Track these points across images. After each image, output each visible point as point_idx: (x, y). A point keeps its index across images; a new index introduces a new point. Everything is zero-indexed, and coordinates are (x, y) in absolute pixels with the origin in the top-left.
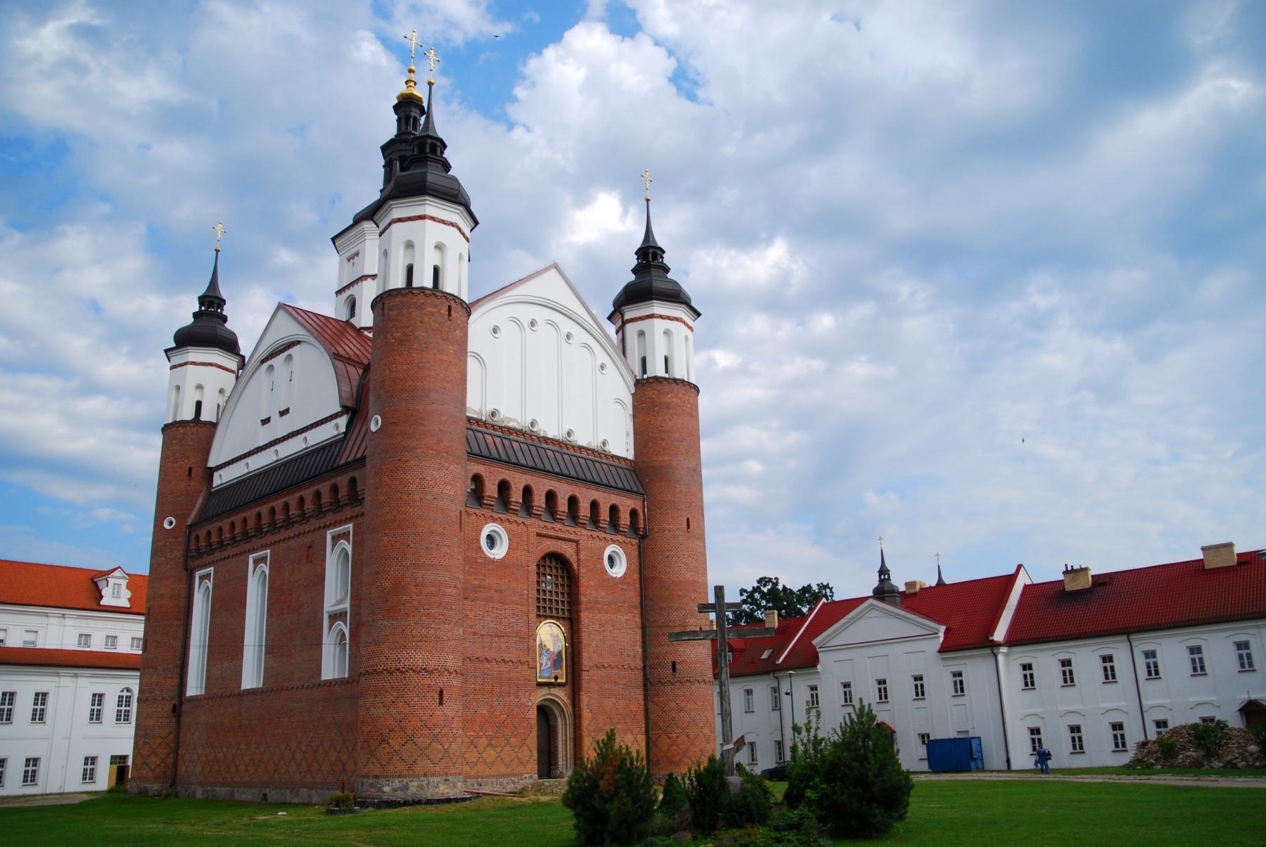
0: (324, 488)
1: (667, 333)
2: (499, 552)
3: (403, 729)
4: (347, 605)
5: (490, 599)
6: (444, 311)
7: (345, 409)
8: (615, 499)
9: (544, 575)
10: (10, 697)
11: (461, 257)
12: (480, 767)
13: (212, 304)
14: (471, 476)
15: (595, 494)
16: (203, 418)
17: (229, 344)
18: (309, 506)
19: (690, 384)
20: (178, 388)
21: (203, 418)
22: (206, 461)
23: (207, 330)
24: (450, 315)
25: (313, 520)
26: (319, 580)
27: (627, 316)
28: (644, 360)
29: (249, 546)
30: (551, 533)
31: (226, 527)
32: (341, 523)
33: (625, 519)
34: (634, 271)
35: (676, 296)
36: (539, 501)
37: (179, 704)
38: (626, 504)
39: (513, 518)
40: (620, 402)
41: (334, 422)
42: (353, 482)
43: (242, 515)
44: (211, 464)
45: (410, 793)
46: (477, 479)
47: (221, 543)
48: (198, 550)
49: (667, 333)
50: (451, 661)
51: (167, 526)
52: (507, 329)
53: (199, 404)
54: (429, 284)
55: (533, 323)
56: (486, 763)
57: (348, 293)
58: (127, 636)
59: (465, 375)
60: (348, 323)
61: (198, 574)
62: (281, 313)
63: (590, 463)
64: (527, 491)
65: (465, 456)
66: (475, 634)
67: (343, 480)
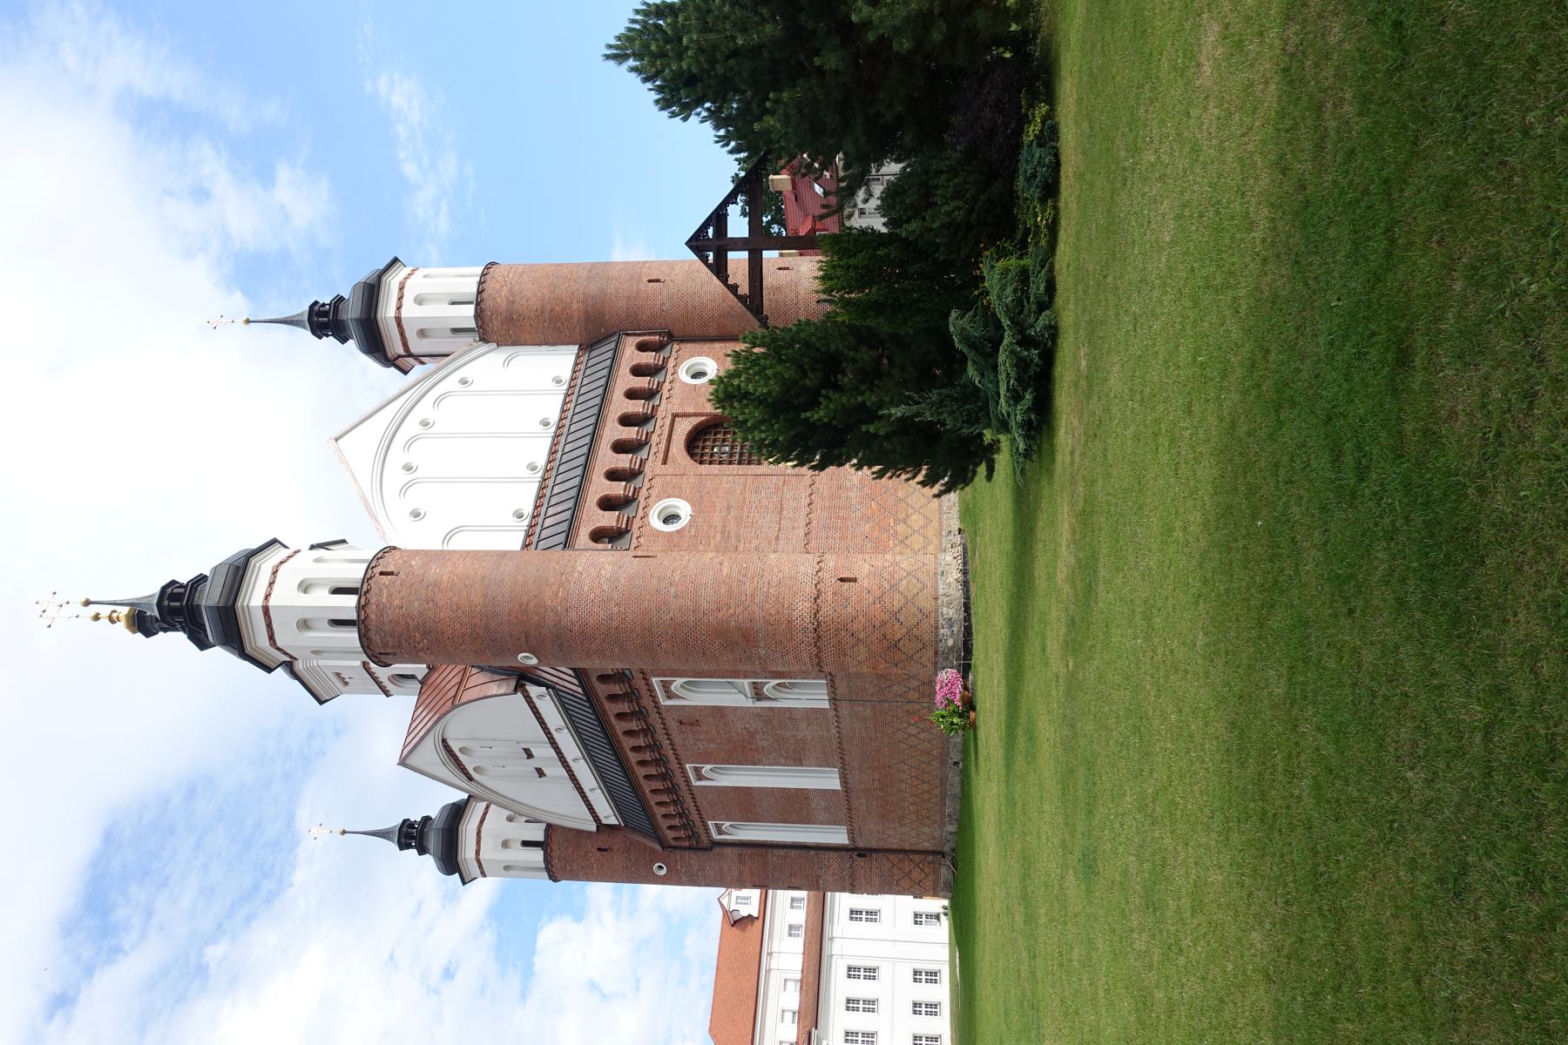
0: (612, 709)
1: (419, 301)
2: (684, 509)
3: (883, 623)
4: (746, 683)
5: (739, 520)
7: (519, 687)
9: (712, 455)
10: (849, 1035)
11: (318, 560)
12: (930, 532)
13: (410, 835)
14: (593, 544)
15: (618, 394)
16: (540, 837)
17: (456, 813)
18: (633, 725)
19: (483, 275)
20: (507, 868)
21: (540, 837)
22: (590, 833)
23: (438, 840)
24: (391, 573)
25: (650, 720)
26: (718, 711)
27: (402, 352)
28: (455, 331)
29: (683, 786)
30: (663, 446)
31: (663, 810)
32: (651, 690)
33: (648, 358)
34: (343, 340)
35: (371, 291)
36: (624, 461)
37: (855, 851)
38: (631, 355)
39: (643, 493)
40: (507, 362)
41: (535, 700)
42: (604, 678)
43: (649, 795)
44: (593, 827)
45: (955, 617)
46: (598, 536)
47: (681, 815)
48: (689, 837)
49: (419, 301)
50: (807, 565)
51: (663, 872)
52: (416, 498)
53: (526, 844)
54: (352, 600)
55: (408, 468)
56: (925, 527)
57: (386, 683)
58: (788, 908)
59: (469, 552)
60: (422, 682)
61: (716, 837)
62: (411, 761)
63: (581, 399)
64: (613, 475)
65: (567, 553)
66: (777, 538)
67: (602, 690)
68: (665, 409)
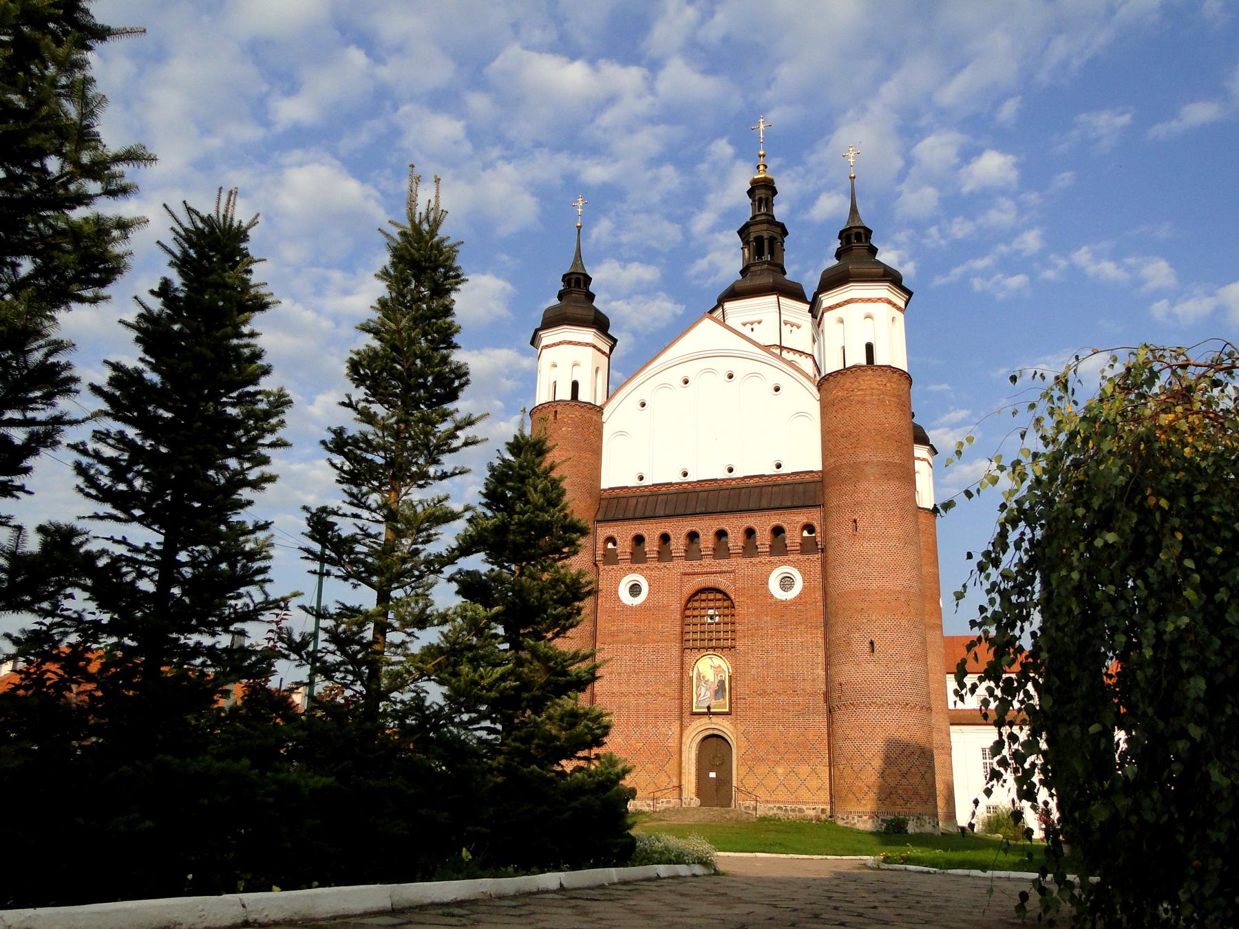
6: (551, 417)
8: (775, 519)
68: (741, 564)
